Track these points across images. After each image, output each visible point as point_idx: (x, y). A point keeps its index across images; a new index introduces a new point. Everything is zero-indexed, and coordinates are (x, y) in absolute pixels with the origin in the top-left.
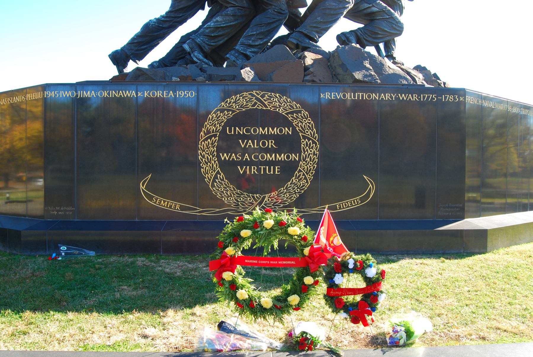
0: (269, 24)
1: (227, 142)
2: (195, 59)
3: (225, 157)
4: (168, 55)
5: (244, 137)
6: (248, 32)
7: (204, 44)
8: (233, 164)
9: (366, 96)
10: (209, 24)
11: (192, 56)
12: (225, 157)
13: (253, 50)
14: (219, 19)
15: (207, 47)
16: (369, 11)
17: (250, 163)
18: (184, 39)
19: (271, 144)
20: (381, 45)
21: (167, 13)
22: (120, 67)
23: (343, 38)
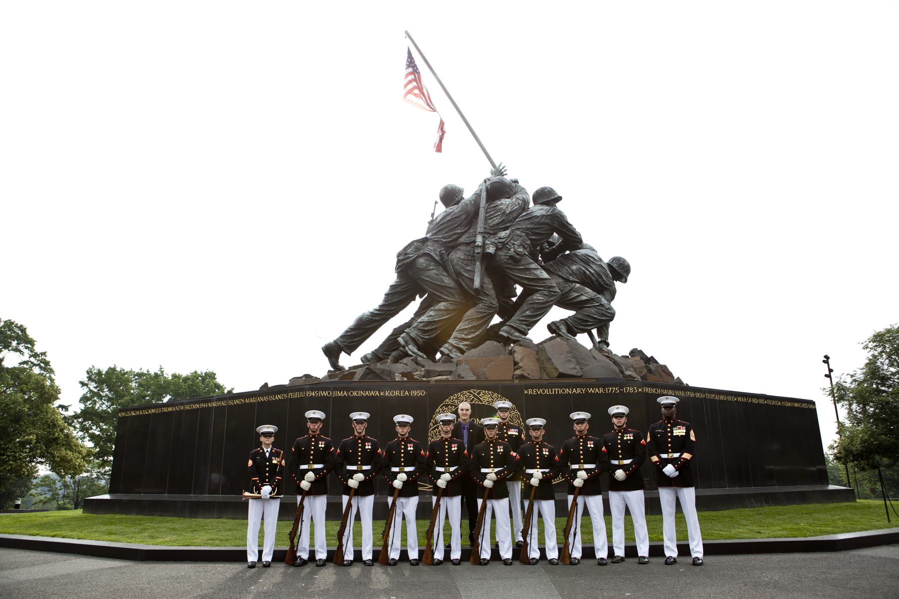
2: (410, 353)
4: (381, 346)
6: (461, 326)
9: (561, 391)
13: (466, 343)
14: (431, 313)
15: (421, 340)
16: (579, 299)
18: (398, 332)
20: (594, 332)
22: (333, 359)
23: (554, 327)
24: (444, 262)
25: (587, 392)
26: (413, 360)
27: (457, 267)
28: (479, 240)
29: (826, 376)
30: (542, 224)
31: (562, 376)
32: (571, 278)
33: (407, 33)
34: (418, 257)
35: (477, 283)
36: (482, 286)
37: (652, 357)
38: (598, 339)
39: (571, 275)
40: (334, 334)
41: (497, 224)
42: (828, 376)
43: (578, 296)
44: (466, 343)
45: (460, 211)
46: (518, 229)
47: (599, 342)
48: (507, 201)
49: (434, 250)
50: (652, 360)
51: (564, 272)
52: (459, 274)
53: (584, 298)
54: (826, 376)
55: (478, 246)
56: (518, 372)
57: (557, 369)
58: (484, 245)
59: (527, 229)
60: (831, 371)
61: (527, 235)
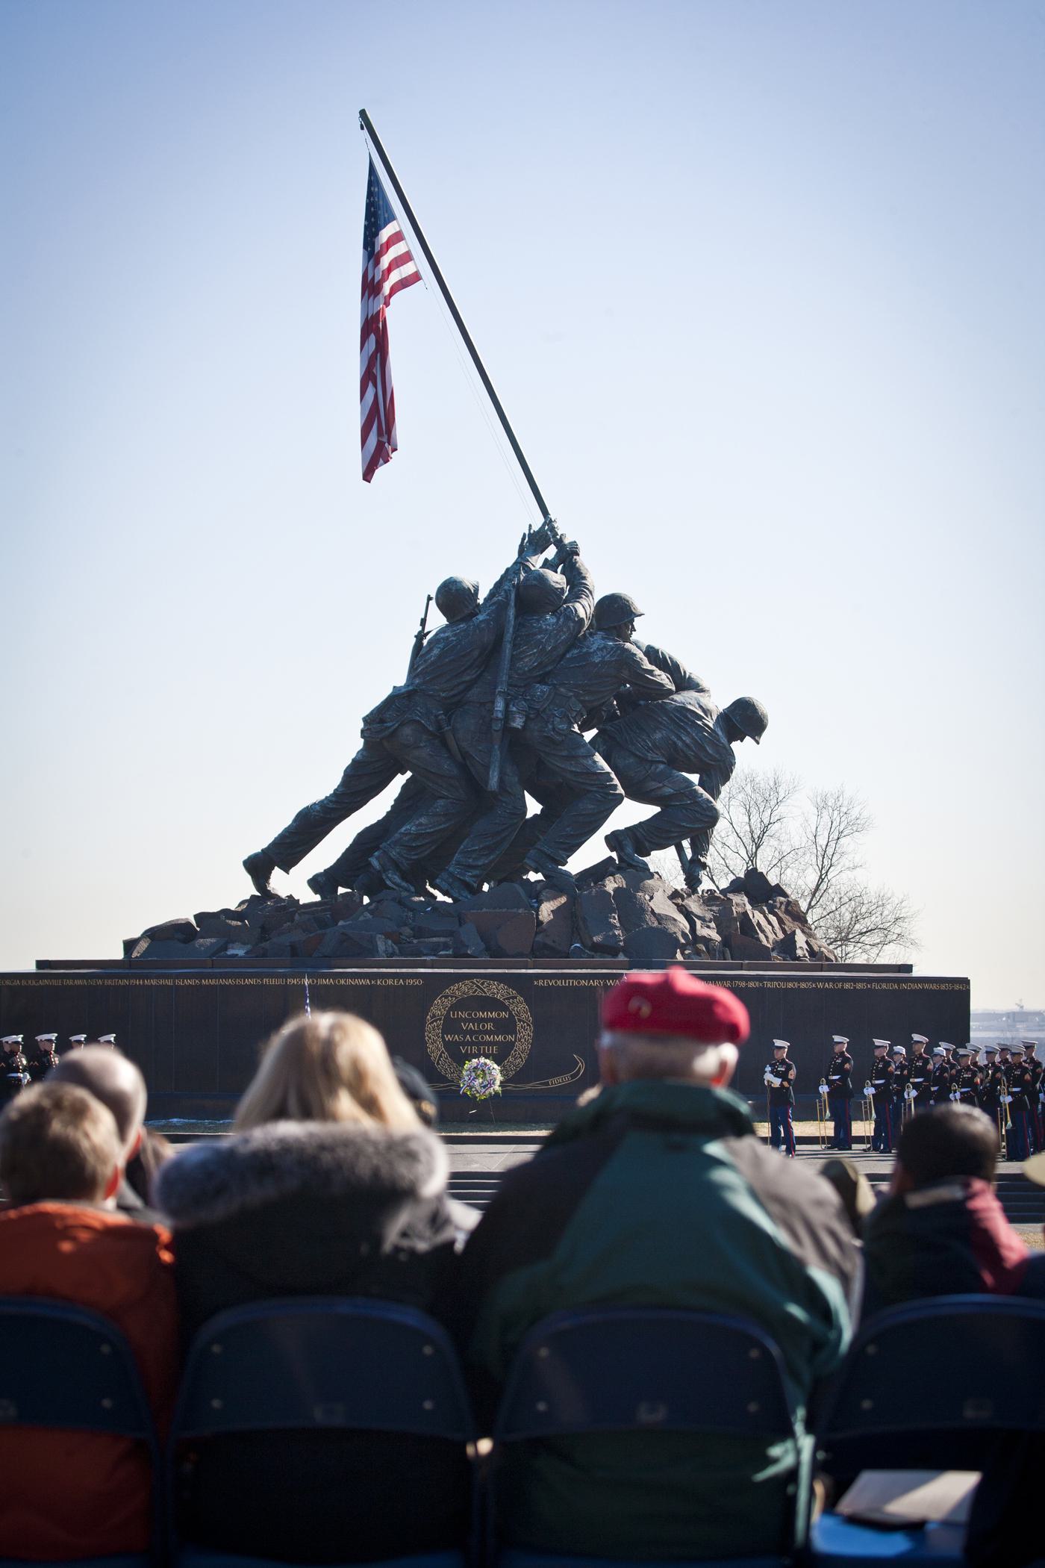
1: (450, 1025)
3: (448, 1038)
5: (465, 1021)
8: (457, 1044)
9: (576, 983)
12: (448, 1038)
14: (423, 820)
17: (472, 1044)
19: (489, 1026)
20: (686, 844)
21: (336, 793)
25: (605, 984)
26: (393, 900)
28: (500, 705)
32: (650, 756)
33: (363, 114)
34: (402, 725)
35: (494, 782)
36: (501, 781)
38: (689, 854)
40: (262, 840)
44: (477, 872)
46: (562, 685)
47: (692, 860)
50: (778, 890)
52: (465, 755)
53: (668, 790)
55: (497, 719)
56: (539, 938)
58: (508, 715)
61: (577, 695)
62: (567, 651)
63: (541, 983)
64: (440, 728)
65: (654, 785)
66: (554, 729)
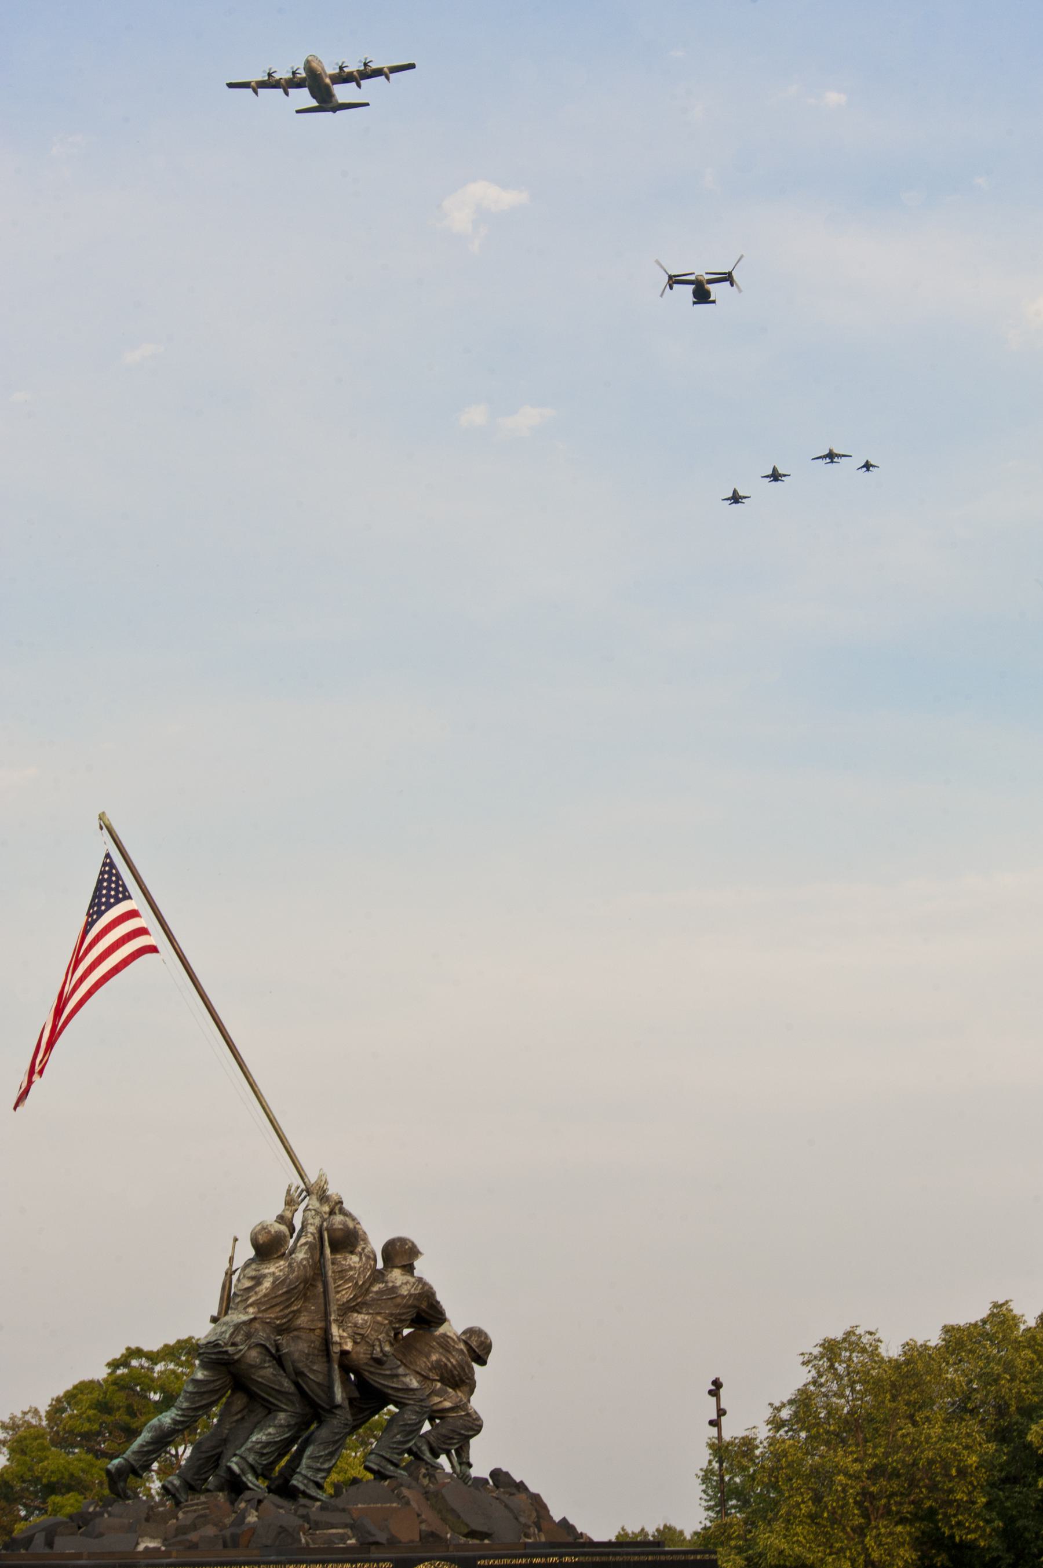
0: (337, 1441)
2: (250, 1485)
7: (256, 1465)
10: (259, 1436)
11: (244, 1479)
14: (271, 1430)
16: (440, 1406)
24: (280, 1356)
25: (531, 1562)
27: (300, 1365)
29: (712, 1423)
30: (409, 1307)
31: (472, 1534)
37: (522, 1482)
39: (430, 1370)
41: (348, 1302)
42: (715, 1423)
43: (440, 1402)
45: (297, 1278)
46: (379, 1314)
48: (355, 1258)
49: (268, 1339)
50: (521, 1487)
51: (422, 1364)
52: (299, 1373)
53: (447, 1404)
54: (712, 1423)
57: (467, 1525)
59: (391, 1315)
60: (721, 1412)
61: (391, 1322)
62: (372, 1285)
63: (482, 1562)
64: (278, 1350)
65: (437, 1399)
66: (382, 1351)
